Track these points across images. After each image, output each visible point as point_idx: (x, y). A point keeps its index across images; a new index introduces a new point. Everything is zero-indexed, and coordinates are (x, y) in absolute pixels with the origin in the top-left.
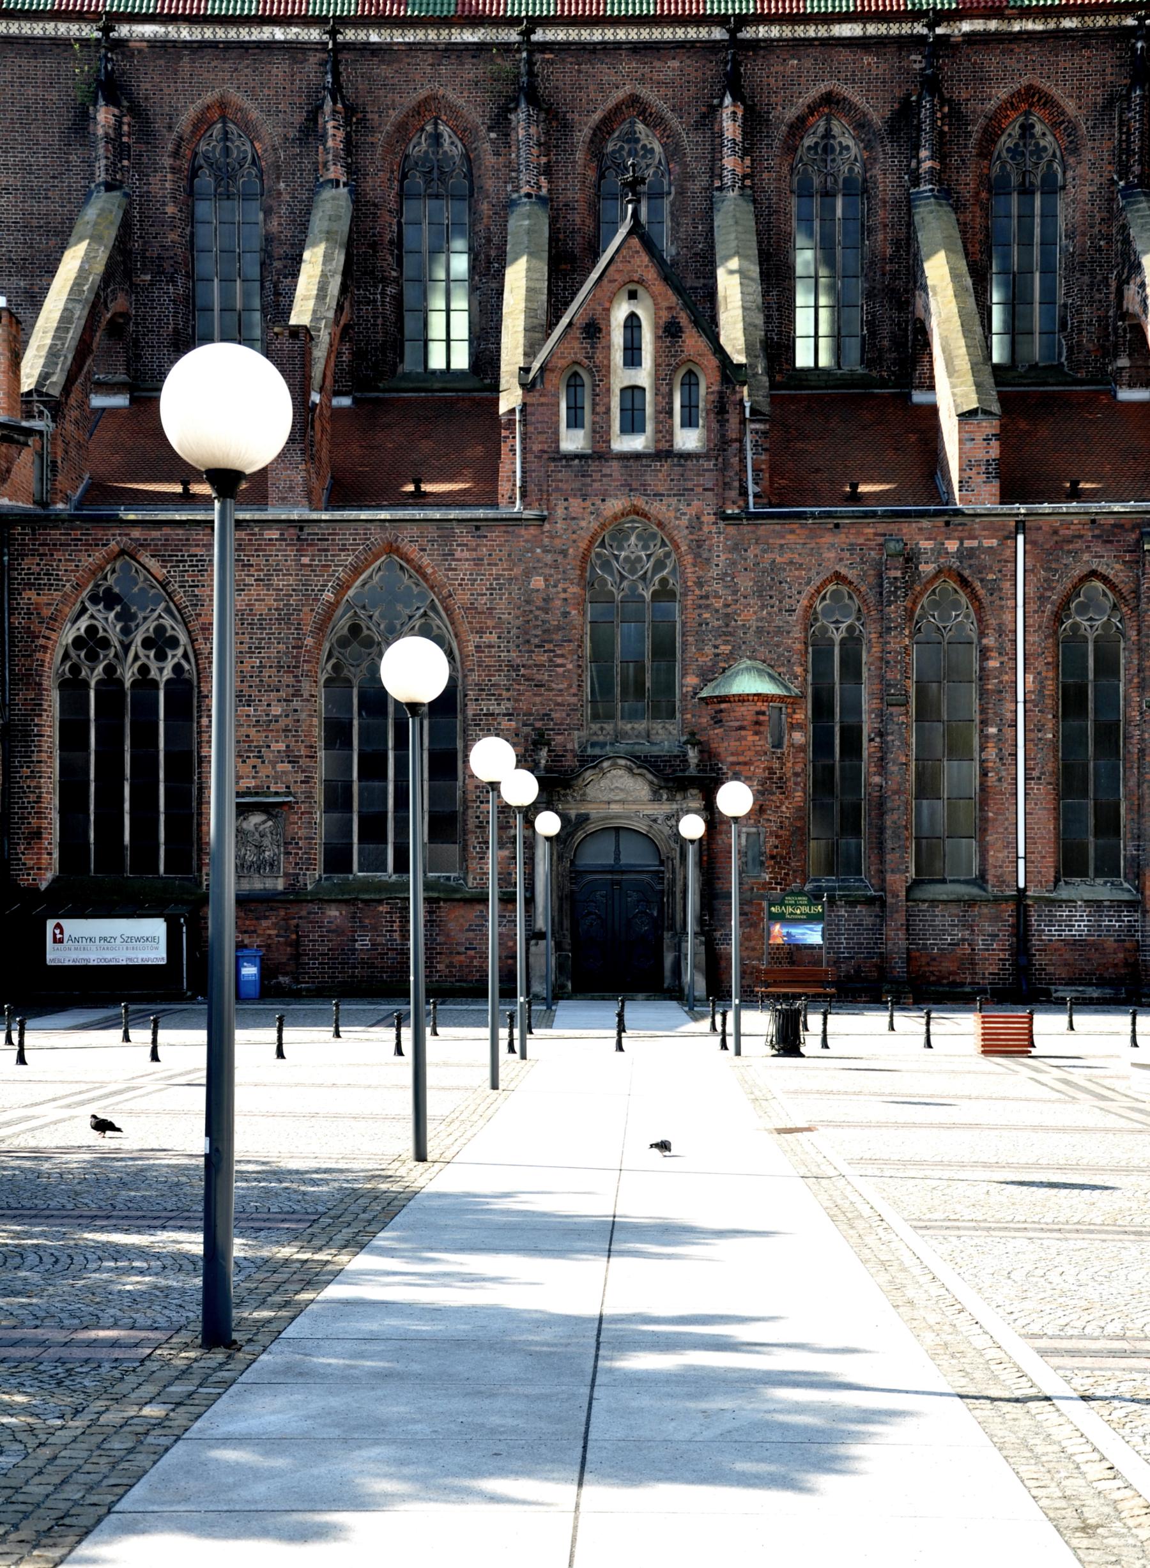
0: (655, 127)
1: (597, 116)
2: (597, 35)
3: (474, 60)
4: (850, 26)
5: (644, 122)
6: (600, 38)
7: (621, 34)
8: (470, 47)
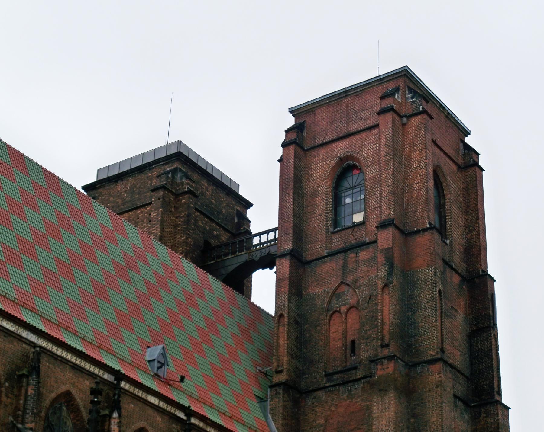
0: (71, 412)
1: (53, 395)
2: (59, 352)
3: (5, 338)
4: (154, 398)
5: (67, 407)
6: (60, 354)
7: (69, 357)
8: (5, 330)
